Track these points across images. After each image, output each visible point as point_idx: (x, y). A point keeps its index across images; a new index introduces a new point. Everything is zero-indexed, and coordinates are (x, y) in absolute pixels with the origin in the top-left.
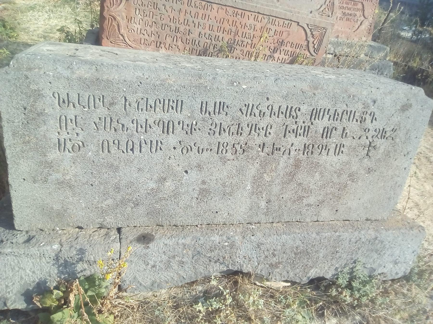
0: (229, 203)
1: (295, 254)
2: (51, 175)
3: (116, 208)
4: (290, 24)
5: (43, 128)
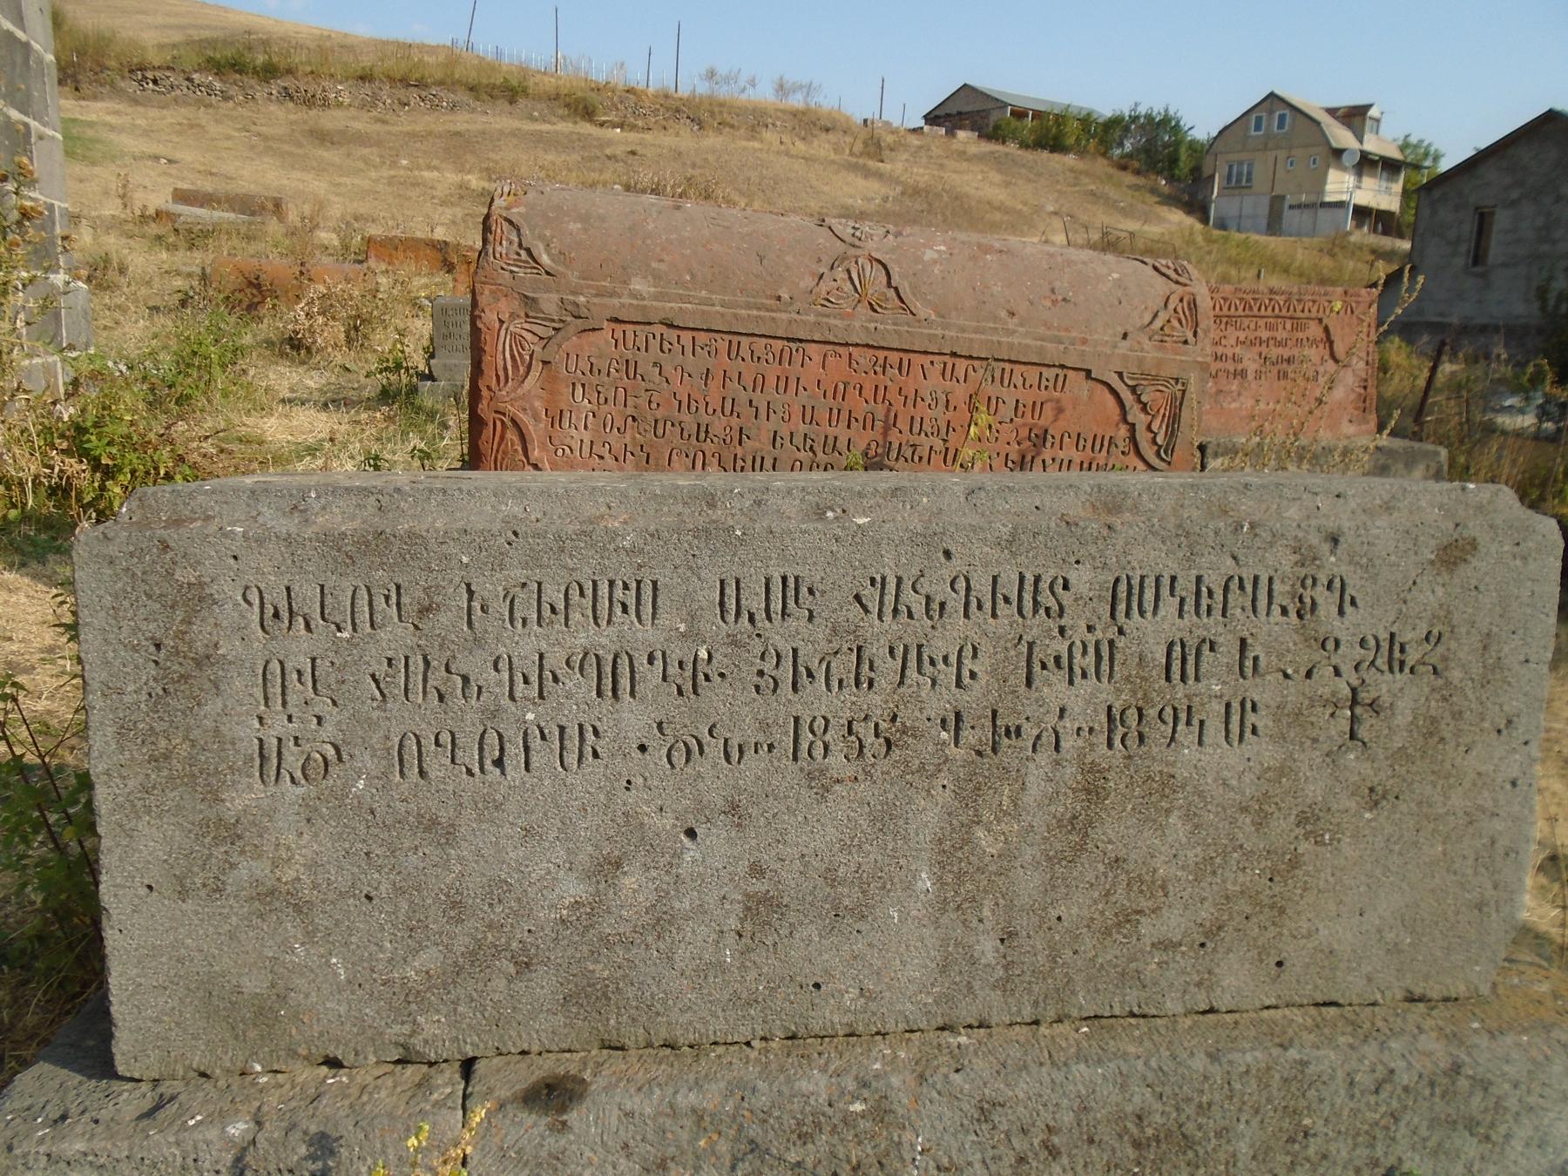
1: (1137, 1145)
2: (233, 866)
3: (454, 982)
4: (1061, 379)
5: (213, 706)
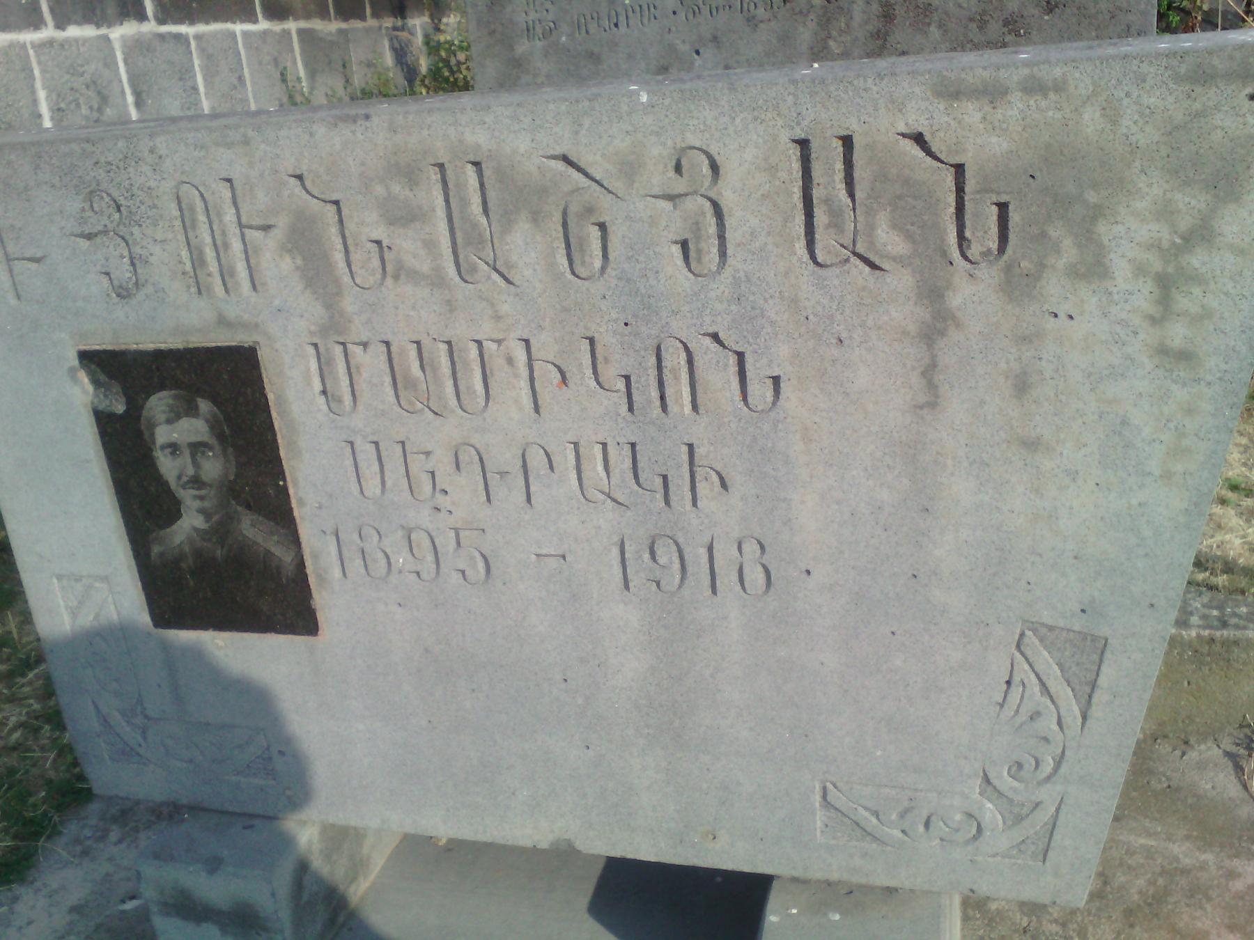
5: (509, 9)
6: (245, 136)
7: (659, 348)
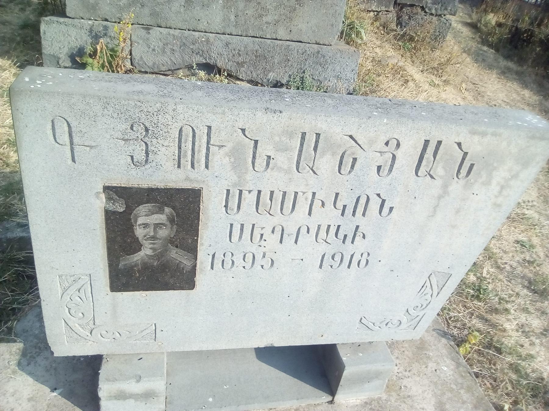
0: (207, 13)
1: (256, 56)
6: (224, 111)
7: (359, 197)
